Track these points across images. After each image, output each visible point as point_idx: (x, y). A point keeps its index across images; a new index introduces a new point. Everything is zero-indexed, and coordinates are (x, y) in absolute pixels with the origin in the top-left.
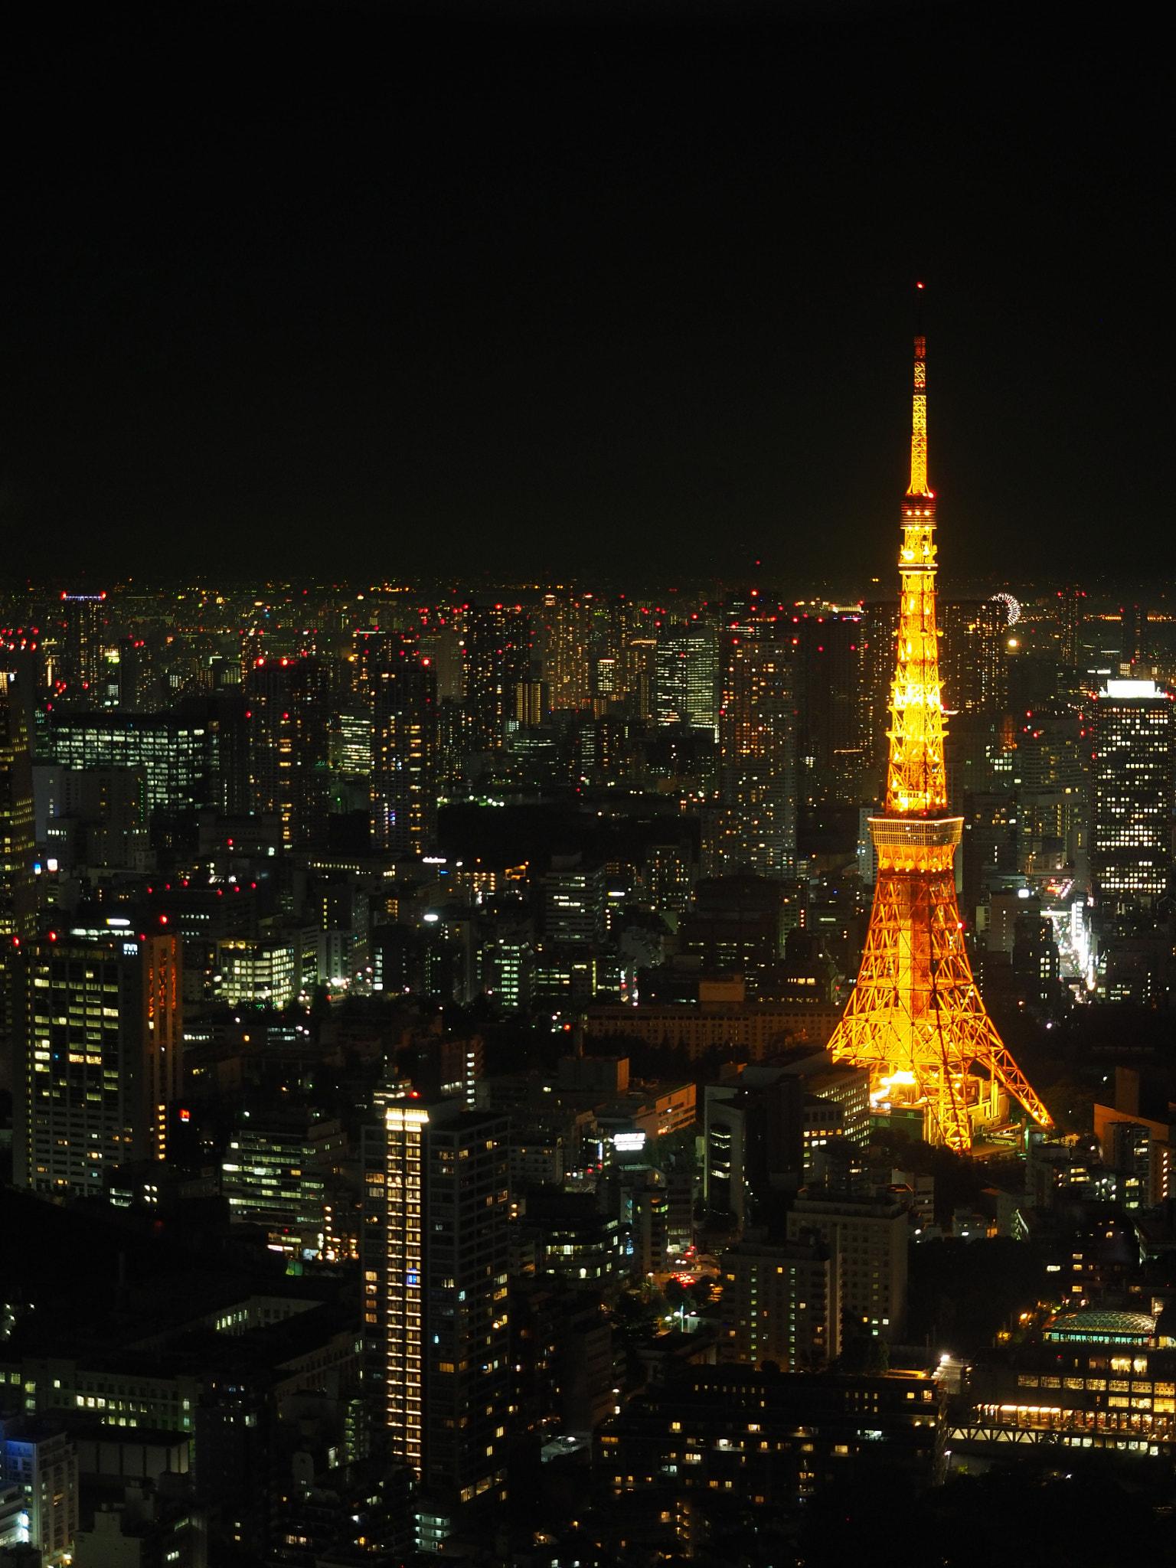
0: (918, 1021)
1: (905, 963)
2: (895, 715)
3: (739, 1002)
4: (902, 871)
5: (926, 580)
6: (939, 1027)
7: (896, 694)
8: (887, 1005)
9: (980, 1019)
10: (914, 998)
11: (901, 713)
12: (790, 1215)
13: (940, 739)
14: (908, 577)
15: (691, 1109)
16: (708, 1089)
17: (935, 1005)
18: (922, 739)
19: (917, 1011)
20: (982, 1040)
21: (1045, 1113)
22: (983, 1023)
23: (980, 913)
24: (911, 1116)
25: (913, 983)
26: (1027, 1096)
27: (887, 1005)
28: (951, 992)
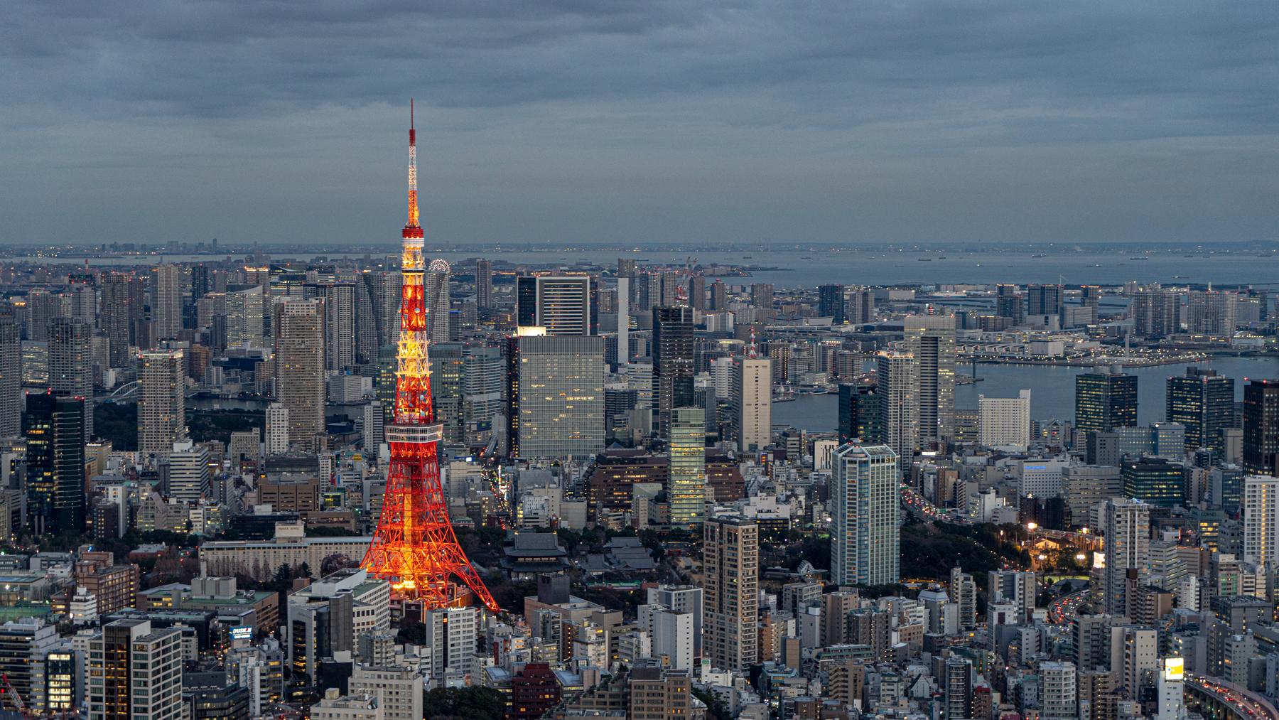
0: (417, 549)
1: (408, 514)
2: (400, 362)
3: (301, 538)
4: (406, 458)
5: (418, 279)
6: (429, 553)
7: (401, 349)
8: (397, 540)
9: (454, 547)
10: (414, 535)
11: (403, 360)
12: (350, 680)
13: (428, 375)
14: (407, 277)
15: (276, 608)
16: (290, 598)
17: (425, 539)
18: (417, 375)
19: (415, 543)
20: (455, 559)
21: (494, 604)
22: (455, 549)
23: (443, 471)
24: (413, 608)
25: (413, 526)
26: (483, 593)
27: (397, 540)
28: (436, 532)
